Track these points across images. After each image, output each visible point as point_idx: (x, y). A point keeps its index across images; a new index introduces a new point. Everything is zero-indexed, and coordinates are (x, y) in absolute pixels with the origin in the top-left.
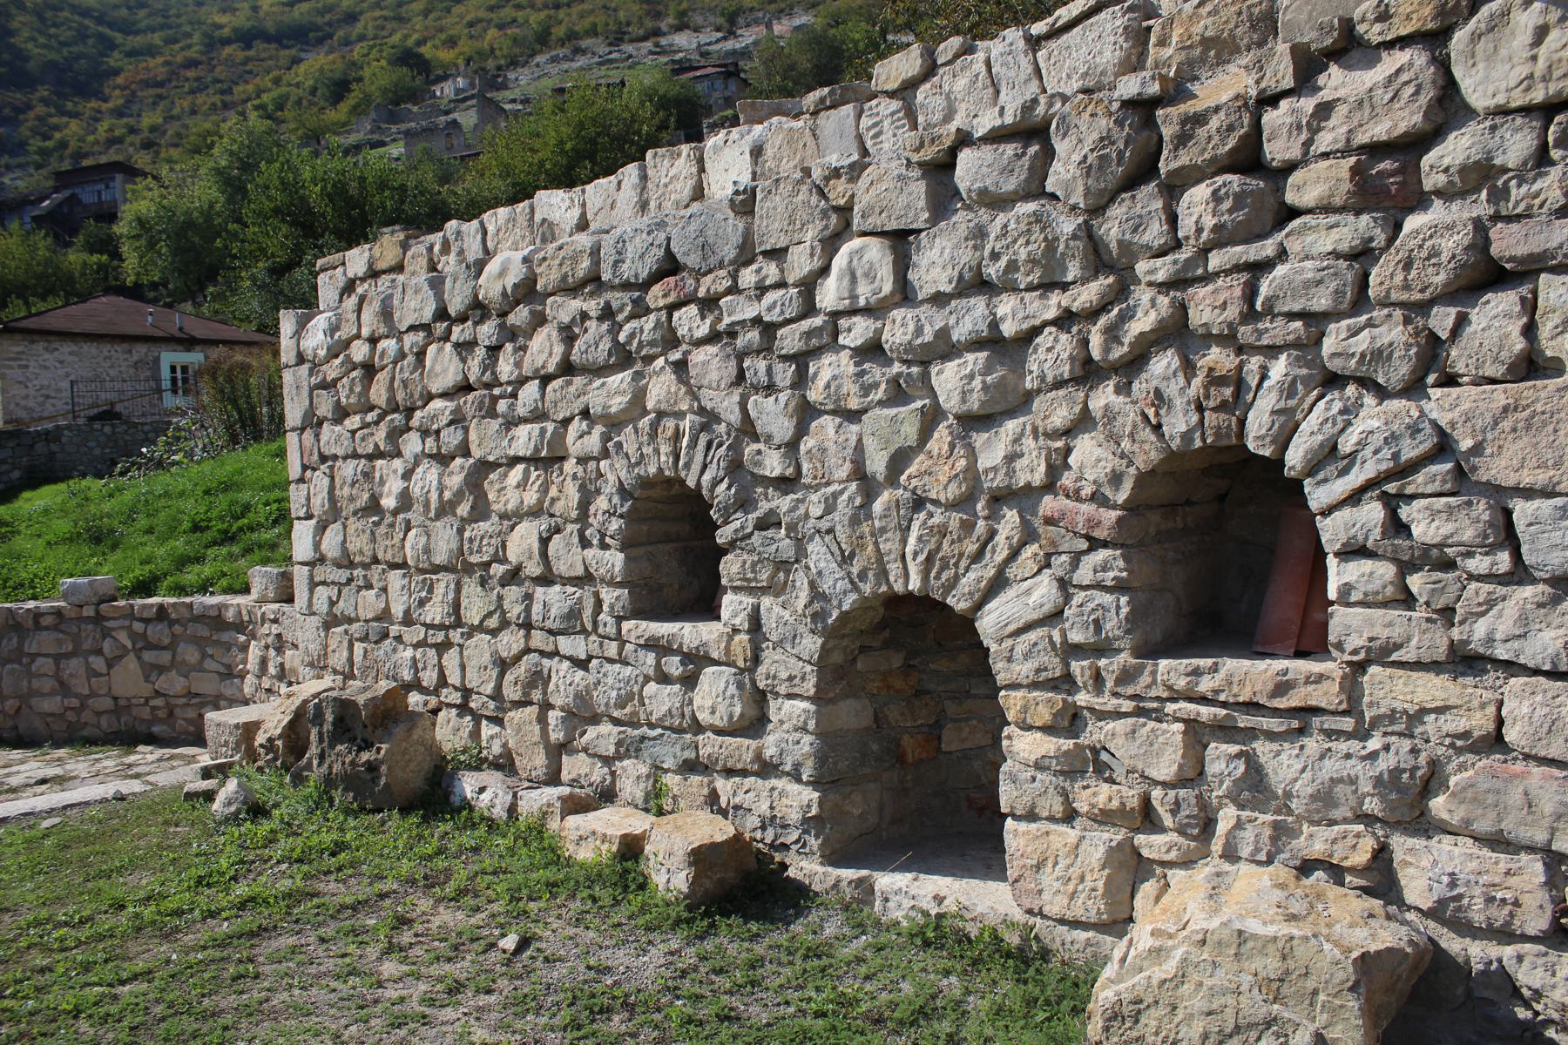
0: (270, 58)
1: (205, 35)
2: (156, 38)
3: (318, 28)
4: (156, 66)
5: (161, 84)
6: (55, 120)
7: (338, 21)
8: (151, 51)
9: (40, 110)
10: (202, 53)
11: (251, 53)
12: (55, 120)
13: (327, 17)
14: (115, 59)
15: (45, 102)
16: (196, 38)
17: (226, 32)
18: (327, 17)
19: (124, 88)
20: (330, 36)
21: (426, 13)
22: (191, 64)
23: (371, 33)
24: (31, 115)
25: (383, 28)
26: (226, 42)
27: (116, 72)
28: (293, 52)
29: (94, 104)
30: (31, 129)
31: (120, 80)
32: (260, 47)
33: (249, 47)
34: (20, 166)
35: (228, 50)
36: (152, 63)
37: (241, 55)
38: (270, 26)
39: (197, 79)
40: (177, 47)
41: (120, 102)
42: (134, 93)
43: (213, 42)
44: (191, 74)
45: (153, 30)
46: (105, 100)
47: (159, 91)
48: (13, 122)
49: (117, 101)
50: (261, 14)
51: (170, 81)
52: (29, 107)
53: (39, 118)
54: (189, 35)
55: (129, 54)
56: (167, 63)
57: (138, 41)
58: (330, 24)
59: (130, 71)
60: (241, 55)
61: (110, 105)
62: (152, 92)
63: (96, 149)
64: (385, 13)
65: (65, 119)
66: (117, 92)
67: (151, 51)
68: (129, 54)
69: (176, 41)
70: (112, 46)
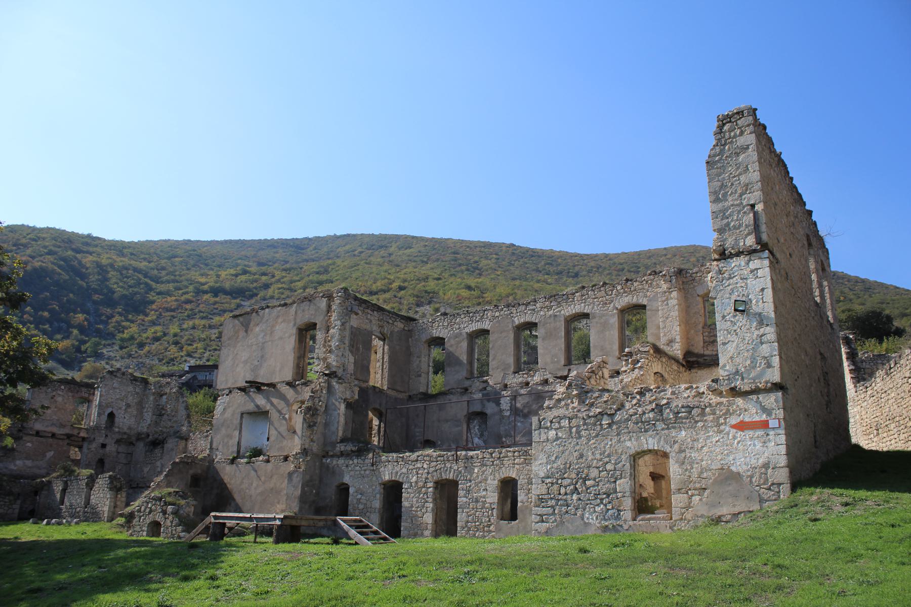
0: (227, 303)
1: (195, 288)
2: (171, 286)
3: (250, 290)
4: (171, 301)
5: (173, 310)
6: (124, 324)
7: (260, 287)
8: (168, 293)
9: (117, 318)
10: (193, 297)
11: (217, 299)
12: (124, 324)
13: (255, 284)
14: (152, 296)
15: (120, 314)
16: (191, 288)
17: (206, 287)
18: (255, 284)
19: (156, 311)
20: (256, 295)
21: (305, 288)
22: (188, 302)
23: (276, 296)
24: (114, 320)
25: (282, 294)
26: (205, 292)
27: (153, 302)
28: (238, 301)
29: (141, 317)
30: (113, 327)
31: (154, 307)
32: (222, 298)
33: (216, 296)
34: (109, 345)
35: (206, 297)
36: (169, 299)
37: (213, 300)
38: (227, 285)
39: (192, 310)
40: (181, 292)
41: (155, 317)
42: (160, 314)
43: (199, 292)
44: (188, 306)
45: (169, 282)
46: (147, 315)
47: (172, 313)
48: (106, 323)
49: (152, 316)
50: (221, 279)
51: (178, 309)
52: (113, 316)
53: (117, 322)
54: (187, 287)
55: (158, 294)
56: (177, 300)
57: (162, 287)
58: (256, 288)
59: (160, 301)
60: (213, 300)
61: (149, 318)
62: (169, 314)
63: (148, 341)
64: (283, 285)
65: (128, 323)
66: (153, 312)
67: (168, 293)
68: (158, 294)
69: (180, 289)
70: (150, 289)
